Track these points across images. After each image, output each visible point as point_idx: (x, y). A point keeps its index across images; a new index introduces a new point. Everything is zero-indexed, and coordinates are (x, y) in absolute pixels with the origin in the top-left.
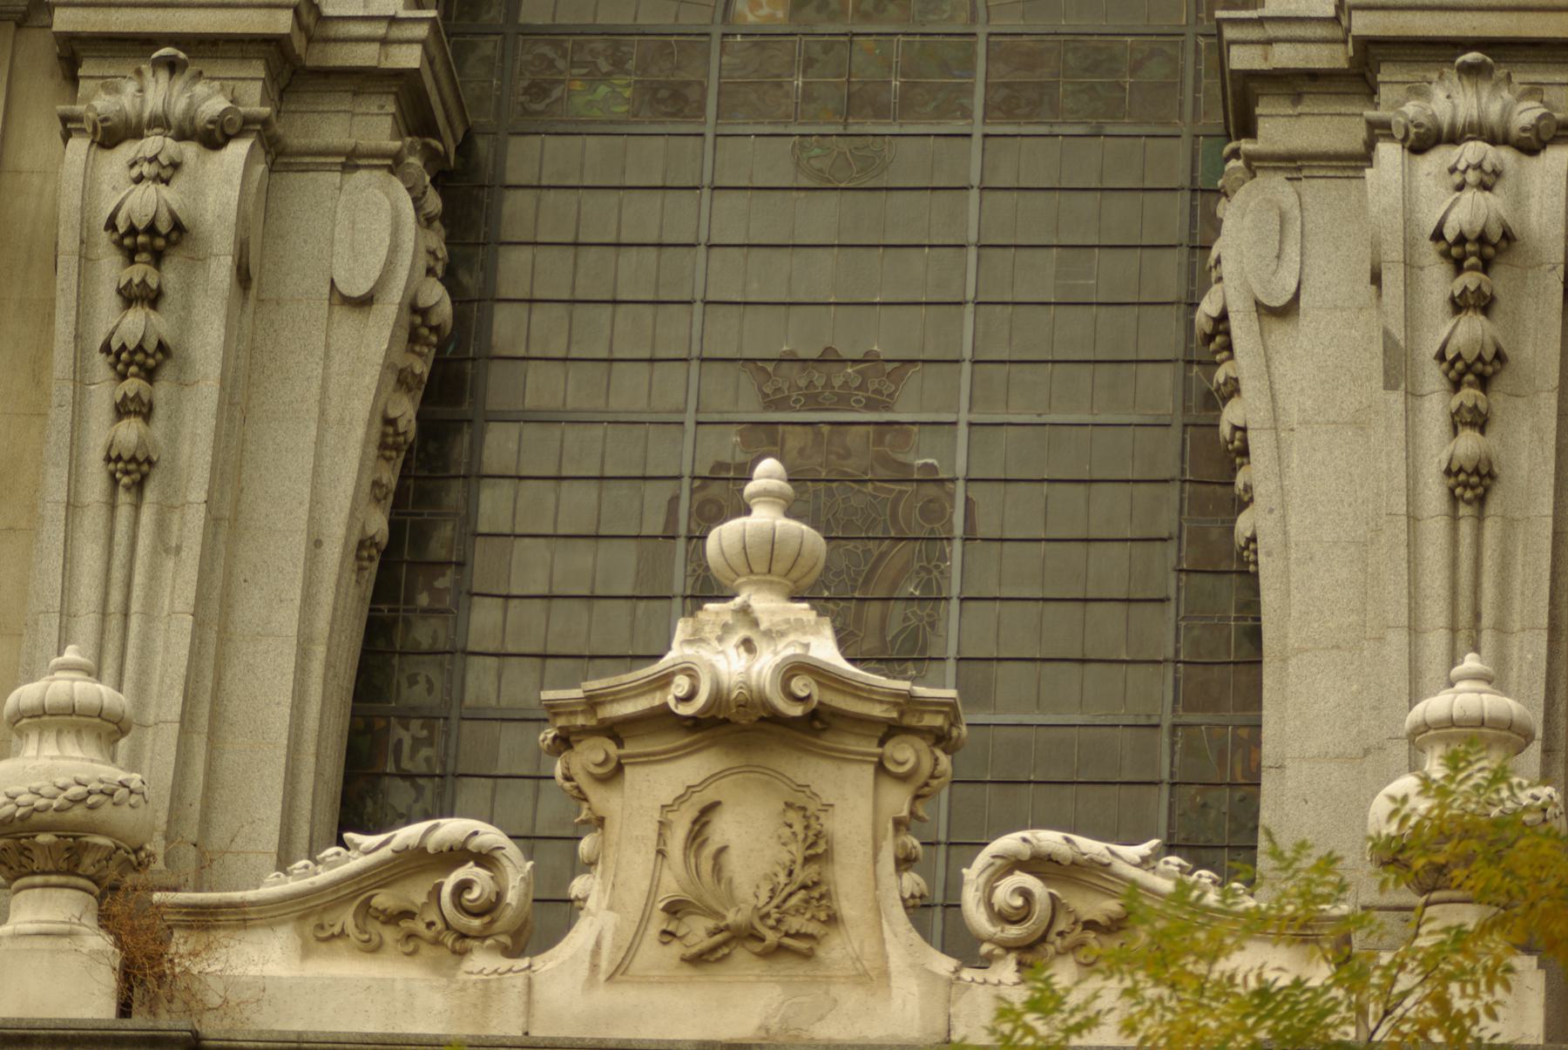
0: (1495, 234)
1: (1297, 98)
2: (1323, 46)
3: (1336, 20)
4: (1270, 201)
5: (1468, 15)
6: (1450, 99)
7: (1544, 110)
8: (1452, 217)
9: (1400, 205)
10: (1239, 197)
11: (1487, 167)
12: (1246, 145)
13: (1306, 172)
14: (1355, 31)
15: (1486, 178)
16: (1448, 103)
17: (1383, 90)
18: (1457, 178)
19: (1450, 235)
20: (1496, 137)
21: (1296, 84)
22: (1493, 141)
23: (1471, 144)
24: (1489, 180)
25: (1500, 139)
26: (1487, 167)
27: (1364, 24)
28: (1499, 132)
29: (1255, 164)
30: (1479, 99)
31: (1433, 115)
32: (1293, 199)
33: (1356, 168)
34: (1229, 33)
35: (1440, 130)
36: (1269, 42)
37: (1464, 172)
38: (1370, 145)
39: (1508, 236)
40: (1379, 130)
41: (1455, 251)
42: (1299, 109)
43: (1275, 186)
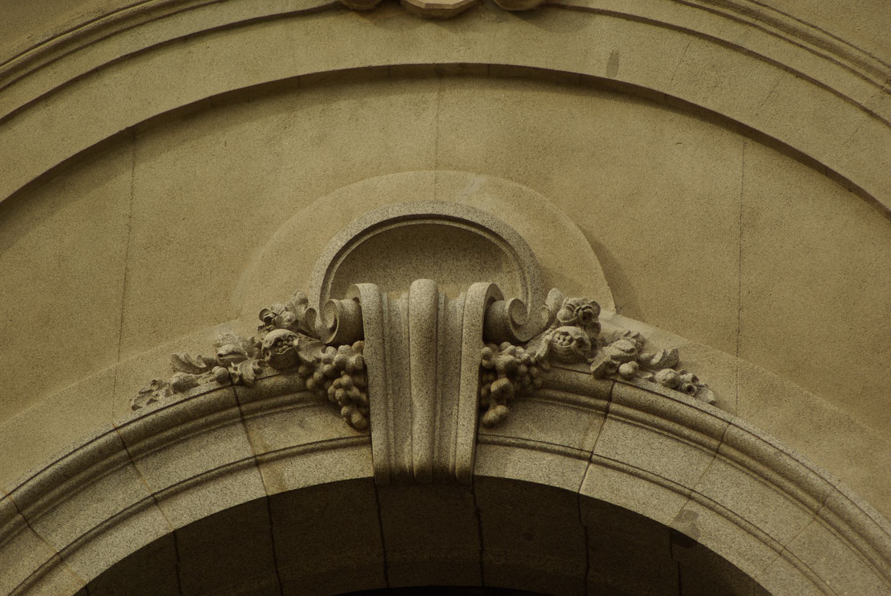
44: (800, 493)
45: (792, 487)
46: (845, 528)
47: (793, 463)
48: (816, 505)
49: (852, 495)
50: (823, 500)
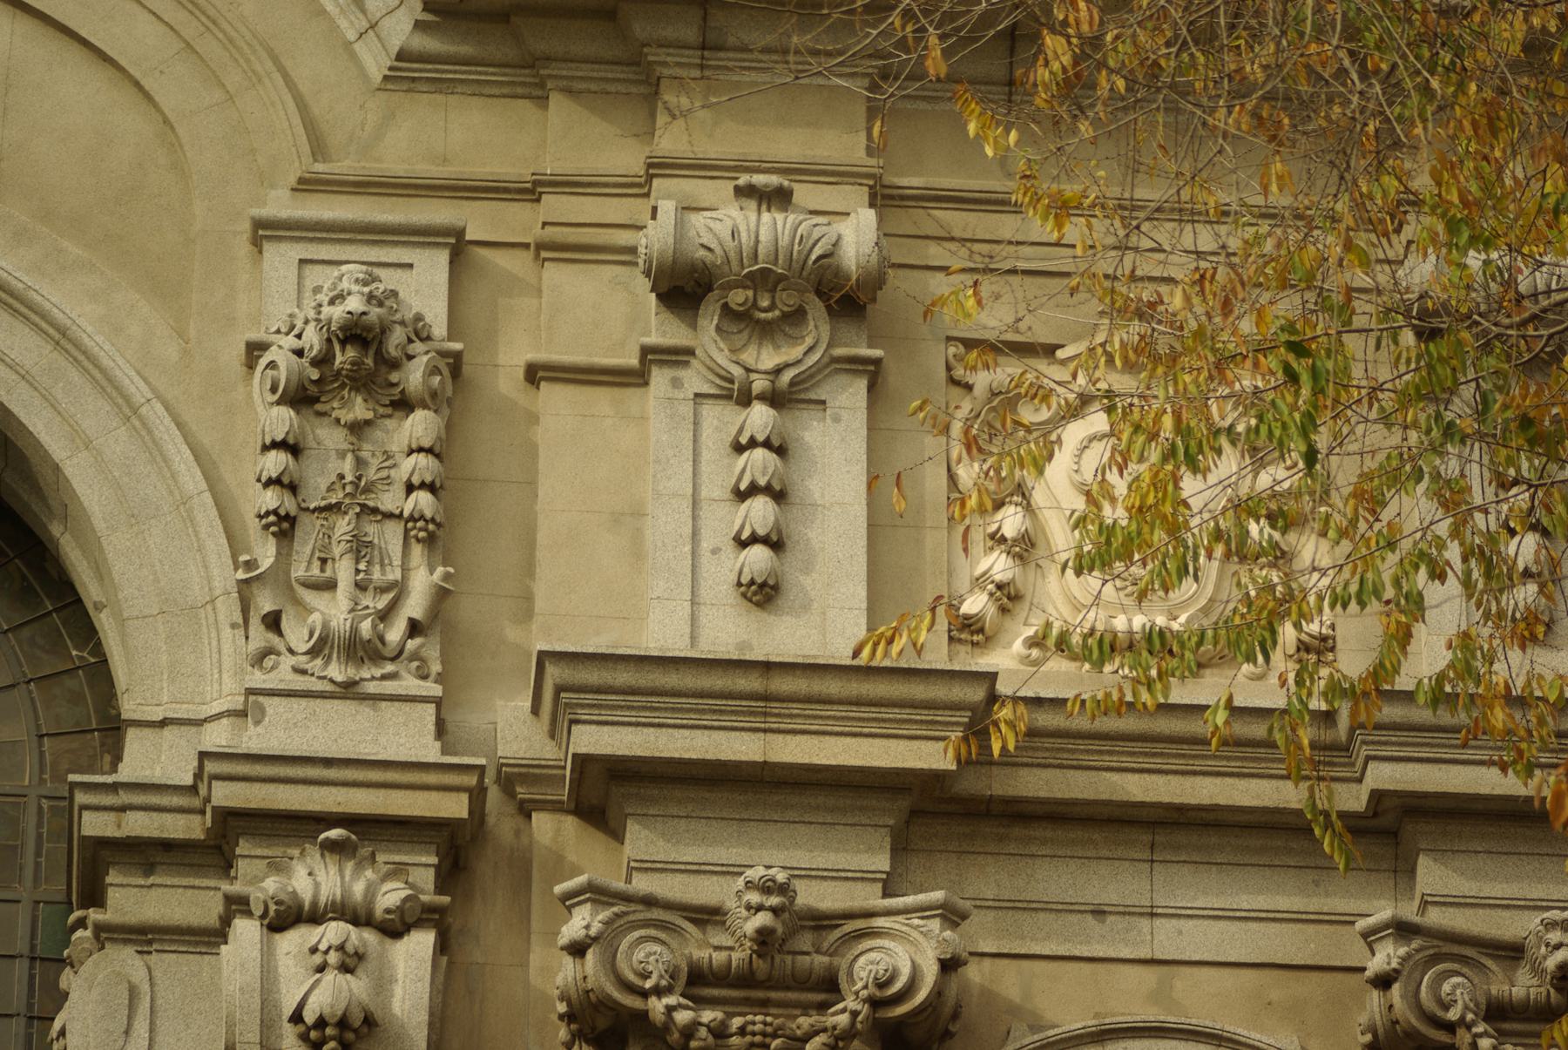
0: (356, 1020)
1: (149, 869)
2: (179, 816)
3: (193, 789)
4: (119, 974)
5: (334, 790)
6: (312, 876)
7: (410, 892)
8: (312, 999)
9: (258, 985)
10: (87, 968)
11: (350, 948)
12: (94, 915)
13: (155, 946)
14: (215, 801)
15: (348, 960)
16: (309, 880)
17: (241, 863)
18: (318, 959)
19: (309, 1016)
20: (359, 917)
21: (149, 855)
22: (356, 922)
23: (333, 924)
24: (350, 962)
25: (363, 920)
26: (350, 948)
27: (225, 795)
28: (362, 912)
29: (107, 934)
30: (342, 877)
31: (294, 892)
32: (143, 973)
33: (208, 944)
34: (81, 798)
35: (300, 907)
36: (123, 809)
37: (326, 952)
38: (226, 921)
39: (369, 1021)
40: (237, 905)
41: (313, 1034)
42: (151, 880)
43: (126, 959)
44: (44, 325)
45: (37, 319)
46: (81, 358)
47: (39, 298)
48: (57, 336)
49: (89, 329)
50: (63, 332)
